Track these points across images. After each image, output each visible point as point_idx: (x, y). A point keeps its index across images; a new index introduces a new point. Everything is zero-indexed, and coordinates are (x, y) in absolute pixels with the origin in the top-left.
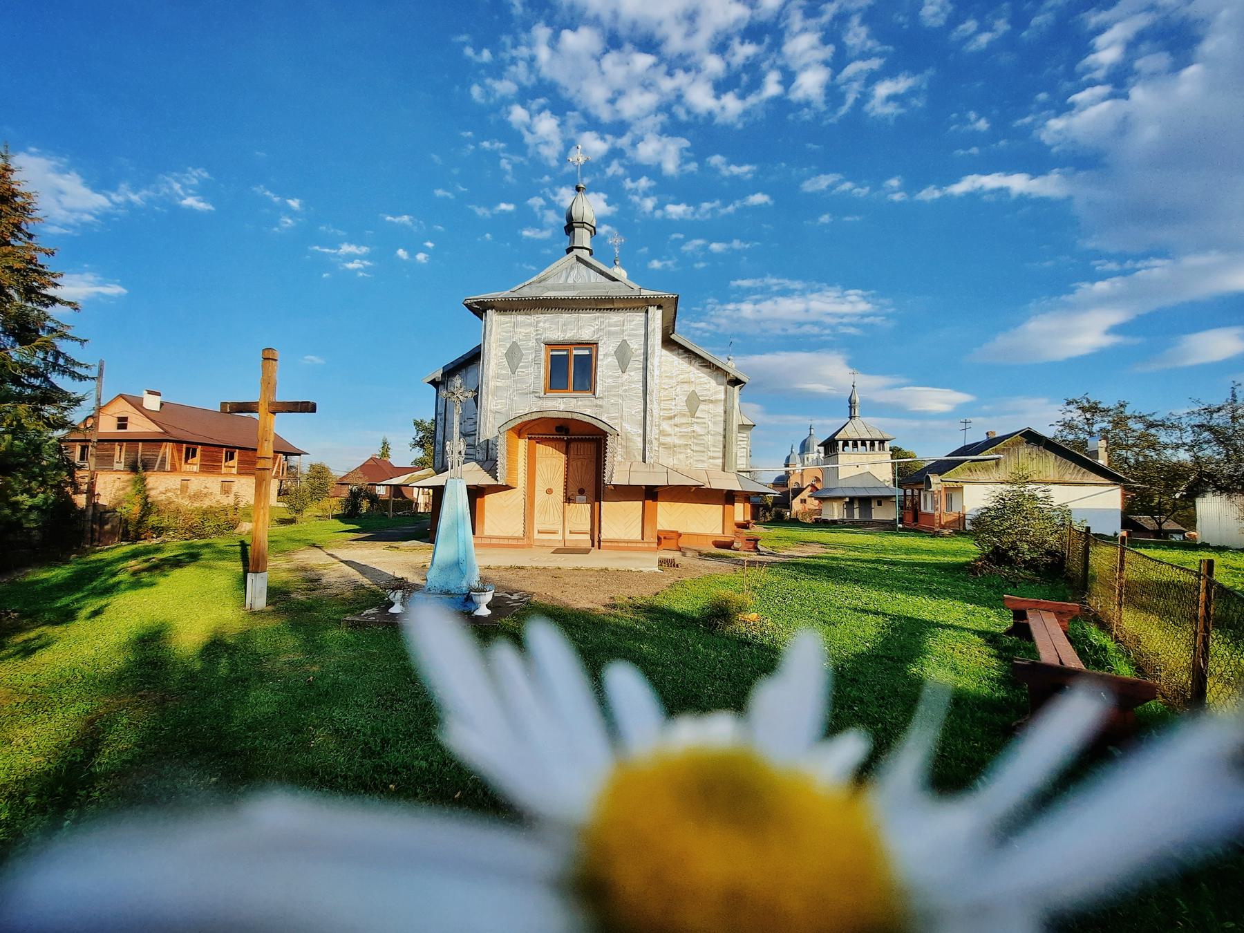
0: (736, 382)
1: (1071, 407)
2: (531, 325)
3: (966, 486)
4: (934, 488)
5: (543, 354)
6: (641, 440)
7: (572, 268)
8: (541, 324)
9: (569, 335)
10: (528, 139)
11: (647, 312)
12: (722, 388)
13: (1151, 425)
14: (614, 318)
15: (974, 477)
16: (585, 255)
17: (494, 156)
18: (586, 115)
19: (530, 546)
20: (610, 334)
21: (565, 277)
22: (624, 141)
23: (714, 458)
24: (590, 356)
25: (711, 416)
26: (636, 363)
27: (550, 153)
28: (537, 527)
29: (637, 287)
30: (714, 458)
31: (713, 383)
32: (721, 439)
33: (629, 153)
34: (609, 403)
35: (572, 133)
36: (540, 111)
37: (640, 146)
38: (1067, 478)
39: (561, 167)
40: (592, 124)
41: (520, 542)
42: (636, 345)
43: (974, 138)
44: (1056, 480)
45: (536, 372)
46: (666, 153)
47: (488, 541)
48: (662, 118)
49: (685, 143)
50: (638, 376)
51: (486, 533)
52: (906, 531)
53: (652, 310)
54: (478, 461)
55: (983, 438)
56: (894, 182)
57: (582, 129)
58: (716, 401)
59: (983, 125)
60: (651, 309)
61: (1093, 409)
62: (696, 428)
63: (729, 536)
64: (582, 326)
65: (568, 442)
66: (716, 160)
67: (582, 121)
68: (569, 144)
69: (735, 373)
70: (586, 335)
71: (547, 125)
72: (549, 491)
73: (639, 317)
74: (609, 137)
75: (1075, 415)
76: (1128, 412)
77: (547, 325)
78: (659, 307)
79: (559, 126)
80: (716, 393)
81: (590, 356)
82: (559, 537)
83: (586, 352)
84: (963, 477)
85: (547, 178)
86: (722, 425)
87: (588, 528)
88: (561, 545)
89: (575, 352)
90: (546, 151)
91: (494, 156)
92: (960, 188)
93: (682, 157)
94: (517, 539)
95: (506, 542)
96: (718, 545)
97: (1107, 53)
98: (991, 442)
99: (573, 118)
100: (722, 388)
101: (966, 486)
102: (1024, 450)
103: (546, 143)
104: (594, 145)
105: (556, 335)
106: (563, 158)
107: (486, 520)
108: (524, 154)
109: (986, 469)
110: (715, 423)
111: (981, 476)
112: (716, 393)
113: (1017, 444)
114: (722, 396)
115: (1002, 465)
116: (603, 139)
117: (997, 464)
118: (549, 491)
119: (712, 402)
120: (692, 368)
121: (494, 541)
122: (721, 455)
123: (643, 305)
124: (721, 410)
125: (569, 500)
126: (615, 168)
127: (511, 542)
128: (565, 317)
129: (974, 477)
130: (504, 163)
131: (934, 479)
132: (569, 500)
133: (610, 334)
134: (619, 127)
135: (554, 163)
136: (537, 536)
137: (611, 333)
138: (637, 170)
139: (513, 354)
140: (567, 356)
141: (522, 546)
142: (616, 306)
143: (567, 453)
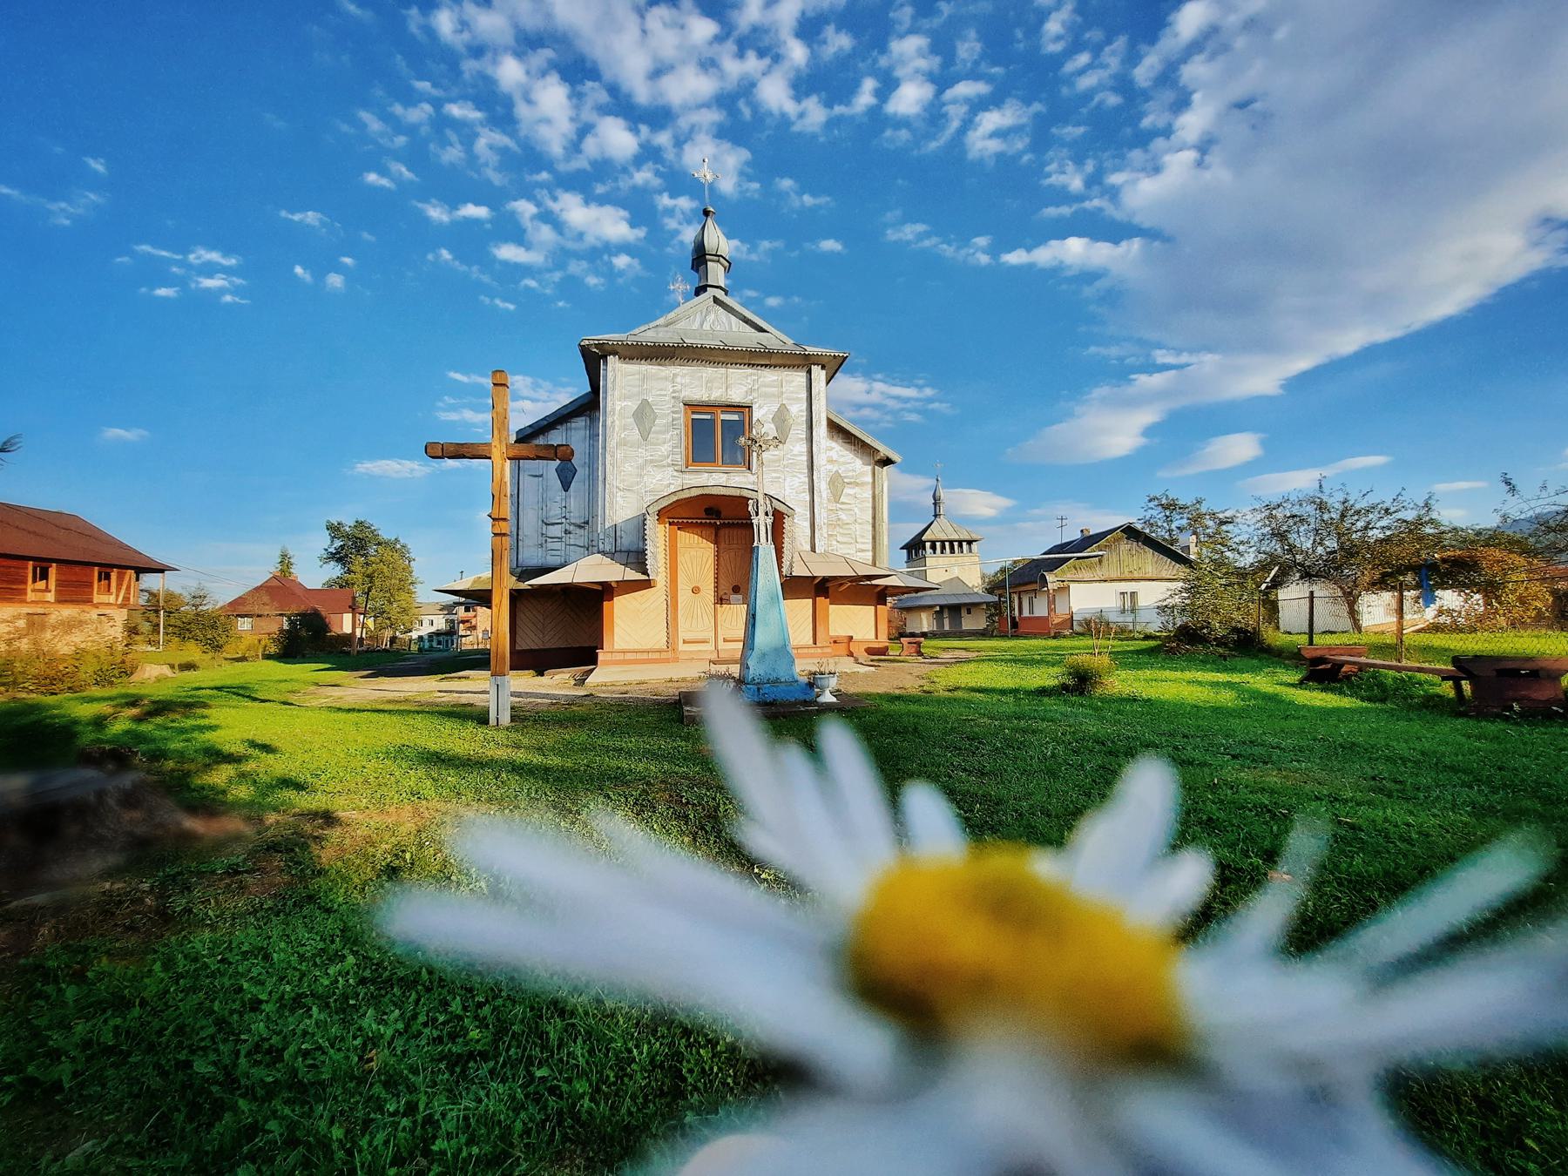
0: (887, 462)
1: (1151, 505)
2: (666, 379)
3: (1072, 585)
4: (1050, 586)
5: (682, 418)
6: (807, 524)
7: (708, 312)
8: (679, 379)
9: (716, 394)
10: (522, 110)
11: (809, 372)
13: (1223, 523)
14: (770, 376)
15: (1079, 576)
16: (720, 294)
17: (467, 133)
18: (613, 90)
19: (676, 660)
20: (766, 396)
21: (701, 321)
22: (663, 139)
24: (741, 422)
25: (858, 501)
26: (799, 431)
27: (554, 138)
28: (682, 635)
29: (790, 342)
32: (870, 528)
33: (670, 155)
34: (773, 478)
35: (588, 115)
36: (543, 74)
37: (687, 147)
38: (1164, 574)
39: (568, 159)
40: (622, 106)
41: (664, 655)
42: (798, 409)
43: (1062, 196)
45: (671, 440)
46: (714, 163)
47: (620, 657)
48: (714, 116)
49: (744, 154)
50: (804, 448)
51: (616, 647)
52: (1004, 636)
53: (816, 370)
54: (604, 553)
55: (1078, 536)
56: (982, 241)
57: (604, 111)
58: (863, 484)
59: (1076, 183)
60: (816, 370)
61: (1171, 506)
62: (843, 517)
63: (883, 641)
64: (733, 385)
65: (717, 528)
66: (787, 183)
67: (603, 97)
68: (585, 130)
69: (885, 451)
70: (736, 397)
71: (553, 97)
73: (799, 377)
74: (644, 129)
75: (1154, 513)
76: (1203, 510)
77: (687, 380)
79: (570, 97)
80: (863, 474)
81: (741, 422)
83: (735, 417)
84: (1069, 576)
85: (544, 176)
86: (870, 512)
87: (741, 634)
88: (714, 657)
89: (723, 417)
90: (544, 132)
91: (467, 133)
92: (1044, 255)
93: (741, 173)
94: (660, 651)
95: (645, 656)
96: (870, 651)
97: (1193, 123)
98: (1088, 541)
99: (596, 93)
101: (1072, 585)
102: (1126, 546)
103: (548, 121)
104: (617, 139)
105: (700, 394)
106: (575, 147)
107: (616, 630)
108: (513, 134)
109: (1090, 567)
110: (861, 510)
111: (1087, 575)
112: (863, 474)
113: (1117, 540)
114: (870, 479)
115: (1105, 562)
116: (634, 130)
118: (696, 590)
119: (857, 484)
120: (834, 444)
121: (629, 656)
122: (870, 547)
123: (805, 362)
124: (868, 494)
125: (720, 600)
126: (643, 176)
127: (651, 656)
128: (709, 372)
129: (1079, 576)
130: (481, 144)
131: (1050, 577)
132: (720, 600)
133: (766, 396)
134: (659, 116)
135: (556, 149)
136: (682, 647)
137: (772, 395)
138: (679, 182)
139: (643, 414)
141: (667, 661)
143: (716, 542)
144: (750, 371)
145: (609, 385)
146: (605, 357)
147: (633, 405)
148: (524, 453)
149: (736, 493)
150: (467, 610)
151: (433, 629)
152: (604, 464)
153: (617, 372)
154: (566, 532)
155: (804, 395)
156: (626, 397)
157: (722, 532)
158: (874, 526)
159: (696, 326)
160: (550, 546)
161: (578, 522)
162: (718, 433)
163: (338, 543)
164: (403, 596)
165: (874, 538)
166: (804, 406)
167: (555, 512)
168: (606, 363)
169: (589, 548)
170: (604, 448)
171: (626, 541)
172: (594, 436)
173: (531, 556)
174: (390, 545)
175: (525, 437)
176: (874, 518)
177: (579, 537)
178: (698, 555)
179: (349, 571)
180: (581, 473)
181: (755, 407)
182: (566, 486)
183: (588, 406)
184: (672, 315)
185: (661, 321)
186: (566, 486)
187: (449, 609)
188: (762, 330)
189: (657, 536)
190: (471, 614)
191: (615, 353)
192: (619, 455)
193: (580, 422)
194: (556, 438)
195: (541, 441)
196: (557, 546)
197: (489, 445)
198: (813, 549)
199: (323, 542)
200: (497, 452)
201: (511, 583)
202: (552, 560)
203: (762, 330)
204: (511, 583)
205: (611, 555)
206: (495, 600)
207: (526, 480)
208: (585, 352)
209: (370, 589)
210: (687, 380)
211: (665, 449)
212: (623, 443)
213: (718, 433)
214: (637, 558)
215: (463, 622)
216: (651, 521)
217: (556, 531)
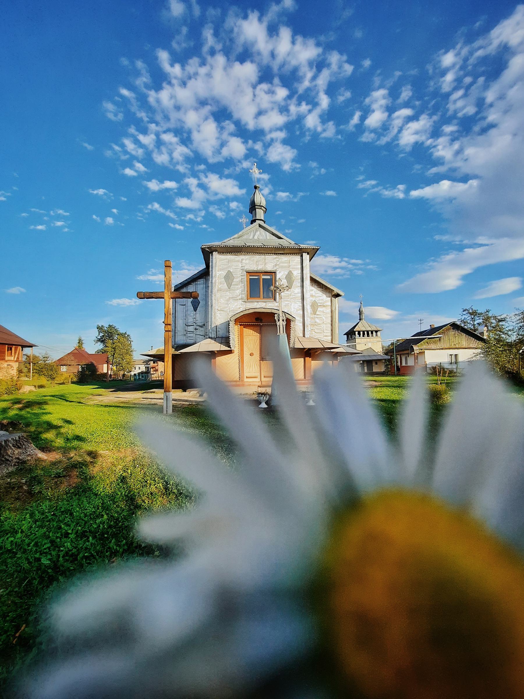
0: (337, 295)
1: (464, 313)
2: (238, 261)
5: (245, 278)
6: (301, 325)
7: (256, 231)
9: (260, 267)
11: (302, 256)
12: (330, 298)
14: (284, 258)
16: (262, 223)
20: (282, 267)
21: (254, 235)
23: (326, 336)
25: (324, 315)
28: (246, 374)
29: (293, 243)
30: (326, 336)
31: (324, 296)
32: (330, 326)
38: (471, 346)
41: (238, 383)
42: (297, 273)
44: (467, 347)
45: (241, 288)
50: (298, 290)
52: (393, 375)
53: (305, 255)
54: (211, 338)
55: (429, 328)
60: (305, 255)
61: (474, 314)
62: (317, 321)
69: (336, 290)
72: (251, 355)
73: (297, 258)
75: (466, 317)
76: (490, 315)
77: (247, 262)
78: (308, 254)
80: (326, 301)
82: (258, 380)
83: (269, 277)
84: (424, 347)
88: (260, 384)
94: (236, 381)
100: (330, 298)
101: (426, 351)
102: (452, 332)
109: (435, 342)
110: (326, 318)
111: (433, 346)
112: (326, 301)
113: (448, 330)
114: (329, 304)
115: (442, 340)
117: (440, 340)
118: (251, 355)
119: (324, 306)
120: (313, 288)
122: (330, 334)
123: (300, 252)
131: (415, 347)
136: (246, 380)
137: (285, 267)
139: (229, 277)
140: (259, 279)
142: (285, 252)
143: (260, 333)
144: (275, 256)
145: (214, 265)
146: (212, 253)
147: (224, 273)
148: (178, 296)
149: (270, 311)
150: (154, 363)
151: (140, 371)
152: (212, 299)
153: (217, 258)
154: (196, 329)
155: (300, 266)
156: (221, 270)
157: (263, 328)
158: (332, 325)
159: (251, 237)
160: (189, 335)
161: (200, 324)
162: (262, 284)
163: (101, 334)
164: (128, 356)
165: (332, 330)
166: (300, 271)
167: (190, 320)
168: (212, 255)
169: (206, 336)
170: (212, 292)
171: (221, 333)
172: (207, 287)
173: (181, 340)
174: (123, 335)
175: (178, 288)
176: (332, 321)
177: (201, 331)
178: (252, 338)
179: (106, 346)
180: (202, 303)
181: (277, 272)
182: (195, 310)
183: (205, 274)
184: (240, 233)
185: (236, 236)
186: (195, 310)
187: (146, 362)
188: (280, 238)
189: (235, 331)
190: (156, 364)
191: (216, 251)
192: (218, 295)
193: (201, 281)
194: (191, 289)
195: (184, 290)
196: (191, 335)
197: (163, 292)
198: (304, 336)
199: (95, 334)
200: (167, 296)
201: (172, 351)
202: (189, 341)
203: (280, 238)
204: (172, 351)
205: (215, 339)
206: (166, 360)
207: (179, 307)
208: (203, 250)
209: (114, 354)
210: (247, 262)
211: (238, 292)
212: (219, 290)
213: (262, 284)
214: (226, 340)
215: (152, 368)
216: (232, 324)
217: (191, 329)
